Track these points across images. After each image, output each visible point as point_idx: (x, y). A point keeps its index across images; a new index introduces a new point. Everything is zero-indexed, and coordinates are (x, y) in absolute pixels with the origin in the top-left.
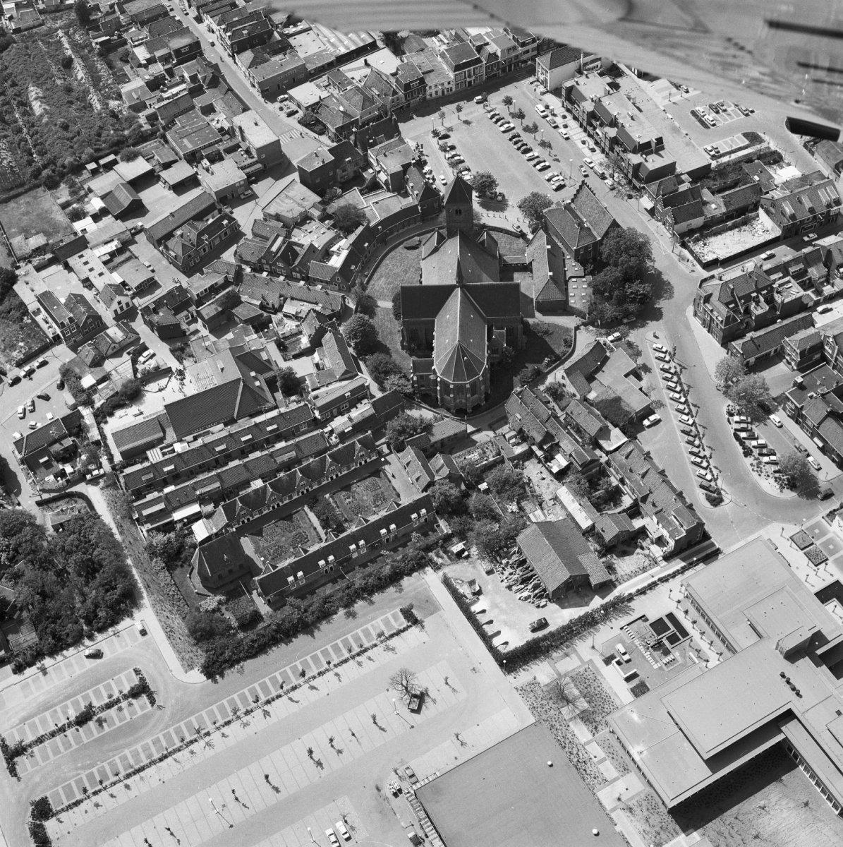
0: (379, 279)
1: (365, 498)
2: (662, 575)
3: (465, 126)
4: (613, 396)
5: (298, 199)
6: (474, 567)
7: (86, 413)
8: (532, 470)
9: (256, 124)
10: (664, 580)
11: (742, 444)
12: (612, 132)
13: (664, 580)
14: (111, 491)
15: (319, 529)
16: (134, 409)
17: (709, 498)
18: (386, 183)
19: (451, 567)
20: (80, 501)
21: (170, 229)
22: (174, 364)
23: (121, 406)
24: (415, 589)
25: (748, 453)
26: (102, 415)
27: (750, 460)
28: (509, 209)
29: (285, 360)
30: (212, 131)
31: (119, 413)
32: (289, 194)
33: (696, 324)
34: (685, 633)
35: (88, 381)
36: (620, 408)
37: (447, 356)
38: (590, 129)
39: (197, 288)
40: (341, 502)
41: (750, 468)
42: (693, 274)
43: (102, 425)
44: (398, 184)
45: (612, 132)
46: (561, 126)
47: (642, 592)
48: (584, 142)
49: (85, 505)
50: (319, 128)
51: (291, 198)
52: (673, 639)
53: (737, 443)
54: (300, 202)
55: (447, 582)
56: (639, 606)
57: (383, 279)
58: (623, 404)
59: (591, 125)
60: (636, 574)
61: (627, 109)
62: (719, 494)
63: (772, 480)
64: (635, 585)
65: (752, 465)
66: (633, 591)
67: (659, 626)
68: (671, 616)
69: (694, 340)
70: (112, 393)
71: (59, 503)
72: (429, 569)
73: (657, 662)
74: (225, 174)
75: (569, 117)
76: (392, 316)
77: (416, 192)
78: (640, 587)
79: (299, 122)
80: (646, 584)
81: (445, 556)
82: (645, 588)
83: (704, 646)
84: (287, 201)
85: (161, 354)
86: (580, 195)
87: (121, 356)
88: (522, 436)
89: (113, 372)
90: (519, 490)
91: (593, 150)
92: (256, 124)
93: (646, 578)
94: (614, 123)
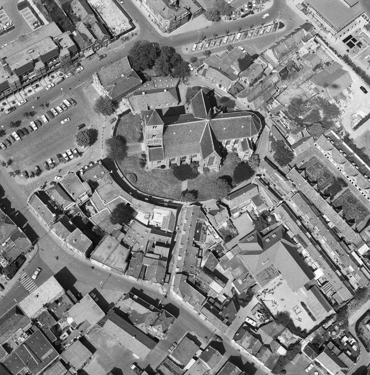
0: (164, 193)
1: (319, 173)
2: (326, 46)
3: (14, 163)
4: (238, 63)
5: (108, 251)
6: (343, 119)
7: (304, 343)
8: (286, 98)
9: (38, 296)
10: (327, 44)
11: (246, 15)
12: (40, 65)
13: (327, 44)
14: (349, 310)
15: (342, 192)
16: (293, 316)
17: (280, 28)
18: (90, 196)
19: (346, 129)
20: (359, 327)
21: (146, 336)
22: (255, 301)
23: (293, 324)
24: (362, 142)
25: (252, 13)
26: (304, 334)
27: (256, 12)
28: (94, 128)
29: (238, 234)
30: (29, 340)
31: (297, 324)
32: (105, 259)
33: (175, 32)
34: (350, 36)
35: (282, 351)
36: (244, 59)
37: (252, 126)
38: (25, 84)
39: (200, 298)
40: (325, 184)
41: (260, 12)
42: (138, 34)
43: (308, 332)
44: (94, 185)
45: (40, 65)
46: (13, 105)
47: (336, 52)
48: (30, 91)
49: (361, 323)
50: (20, 262)
51: (110, 256)
52: (355, 40)
53: (247, 17)
54: (111, 250)
55: (356, 128)
56: (343, 53)
57: (164, 190)
58: (242, 58)
59: (22, 83)
60: (327, 55)
61: (23, 54)
62: (277, 24)
63: (264, 4)
64: (332, 55)
65: (258, 11)
66: (336, 56)
67: (351, 45)
68: (344, 41)
69: (183, 34)
70: (288, 331)
71: (364, 339)
72: (350, 137)
73: (366, 46)
74: (85, 313)
75: (5, 101)
76: (194, 180)
77: (103, 173)
78: (333, 53)
79: (11, 278)
80: (331, 51)
81: (341, 132)
82: (333, 51)
83: (354, 29)
84: (112, 258)
85: (248, 315)
86: (101, 78)
87: (259, 335)
88: (270, 100)
89: (273, 335)
90: (297, 105)
91: (37, 86)
92: (38, 296)
93: (328, 51)
94: (36, 61)
